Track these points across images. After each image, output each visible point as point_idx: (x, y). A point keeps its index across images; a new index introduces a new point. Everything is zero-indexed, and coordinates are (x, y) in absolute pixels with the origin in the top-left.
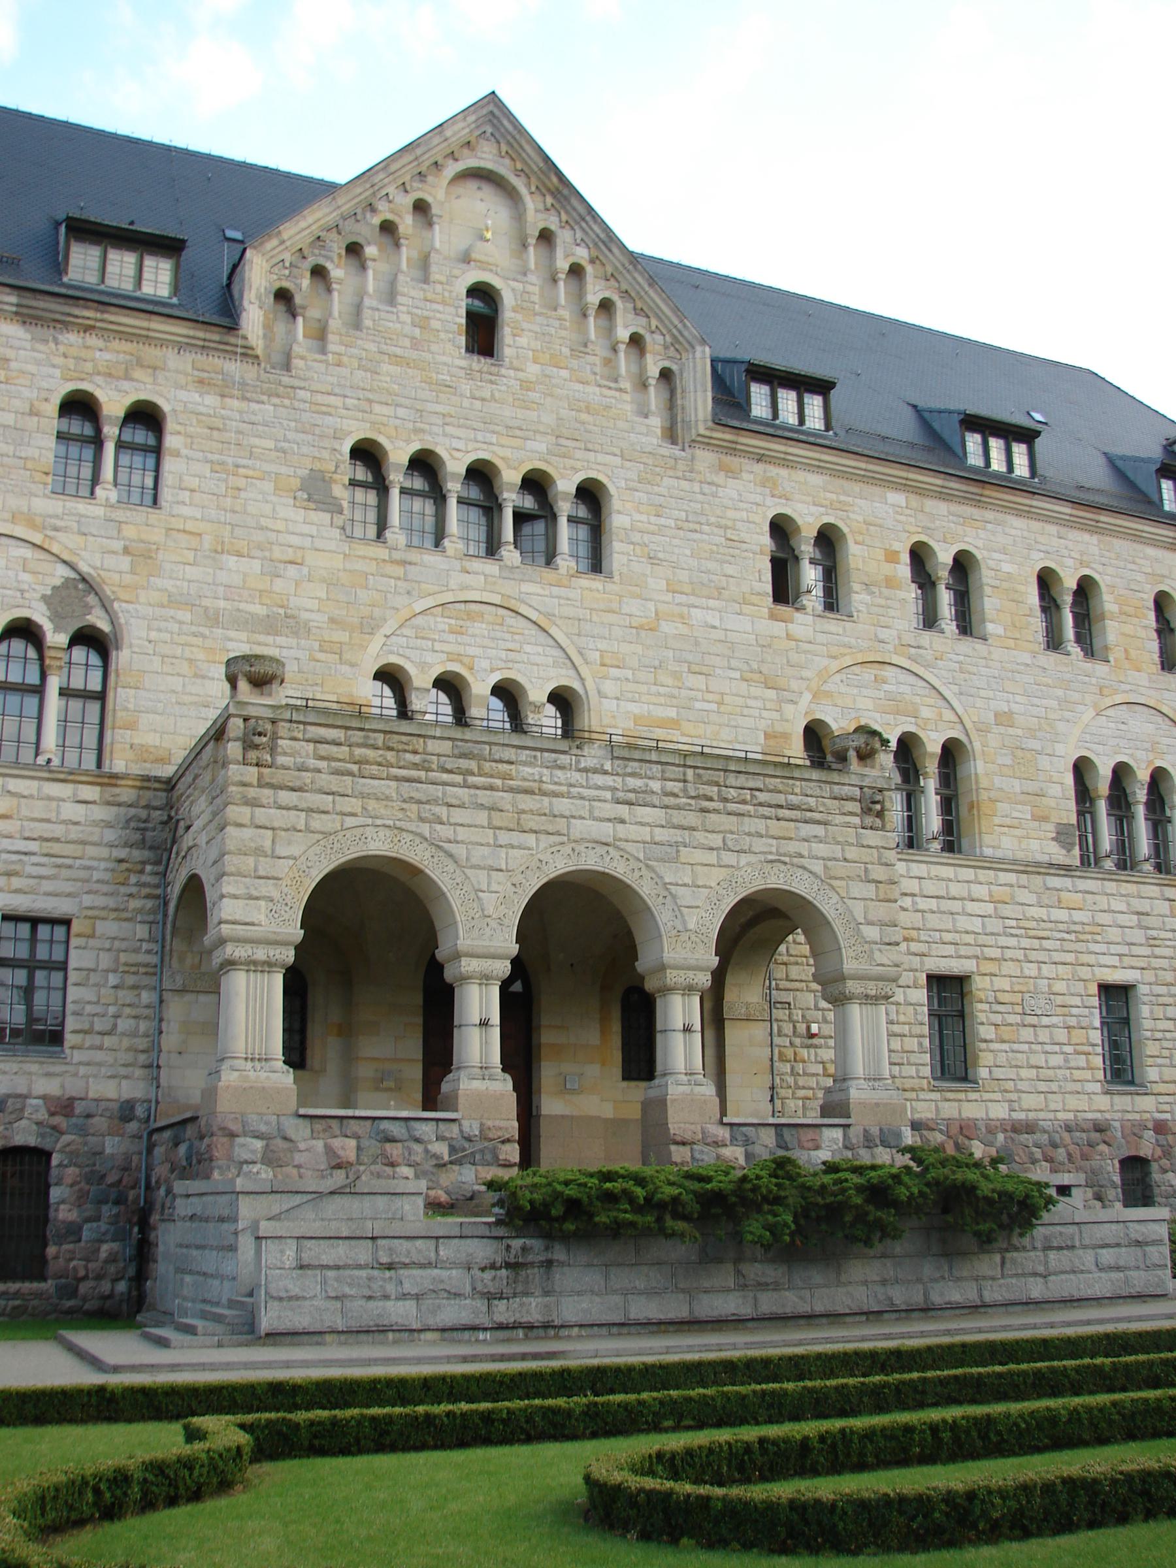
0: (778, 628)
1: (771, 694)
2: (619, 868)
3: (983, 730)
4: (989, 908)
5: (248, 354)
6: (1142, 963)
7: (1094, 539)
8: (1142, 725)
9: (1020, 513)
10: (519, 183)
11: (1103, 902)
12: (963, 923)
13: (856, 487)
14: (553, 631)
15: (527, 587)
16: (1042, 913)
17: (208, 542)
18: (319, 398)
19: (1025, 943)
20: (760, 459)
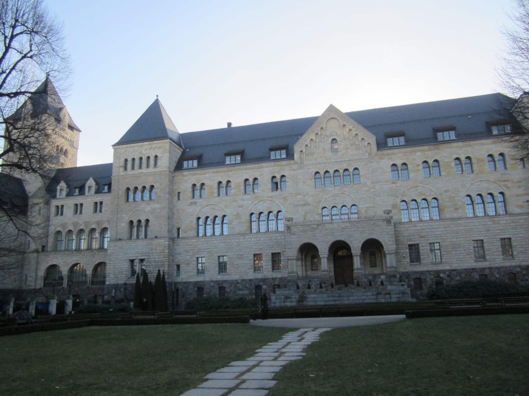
0: (394, 185)
1: (393, 198)
2: (343, 239)
3: (441, 194)
4: (443, 229)
5: (296, 163)
6: (484, 235)
7: (470, 148)
8: (484, 185)
10: (338, 118)
11: (472, 224)
12: (436, 233)
14: (351, 196)
15: (345, 189)
16: (457, 228)
17: (294, 195)
18: (308, 167)
19: (452, 235)
20: (388, 155)
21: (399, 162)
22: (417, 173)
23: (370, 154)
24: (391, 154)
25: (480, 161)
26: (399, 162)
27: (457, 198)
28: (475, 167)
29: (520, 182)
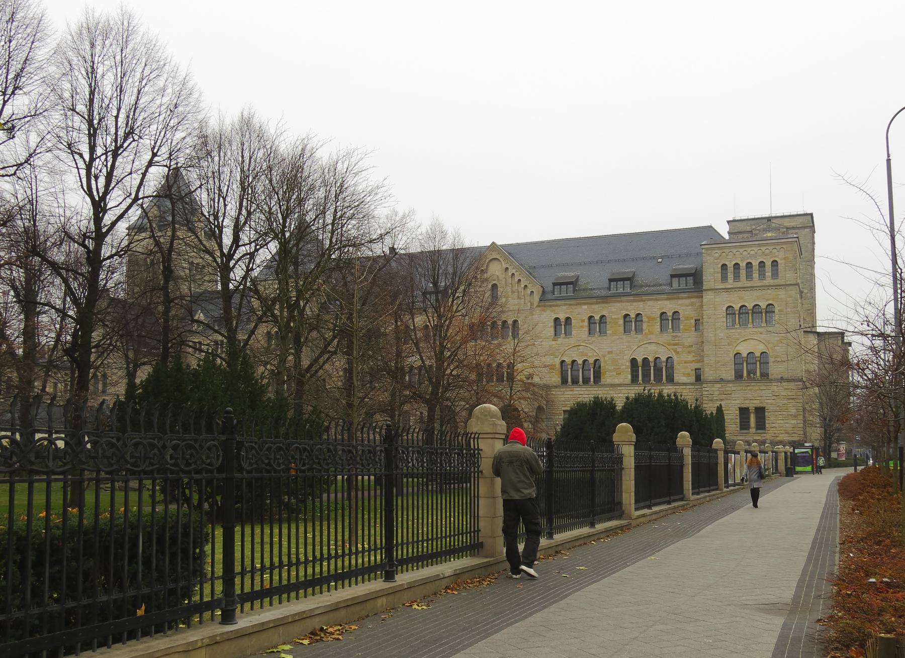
0: (554, 342)
3: (604, 356)
8: (652, 347)
9: (618, 302)
13: (573, 307)
20: (551, 306)
21: (562, 317)
22: (580, 330)
23: (532, 304)
24: (554, 306)
25: (651, 319)
26: (562, 317)
27: (620, 361)
28: (645, 326)
29: (691, 346)
